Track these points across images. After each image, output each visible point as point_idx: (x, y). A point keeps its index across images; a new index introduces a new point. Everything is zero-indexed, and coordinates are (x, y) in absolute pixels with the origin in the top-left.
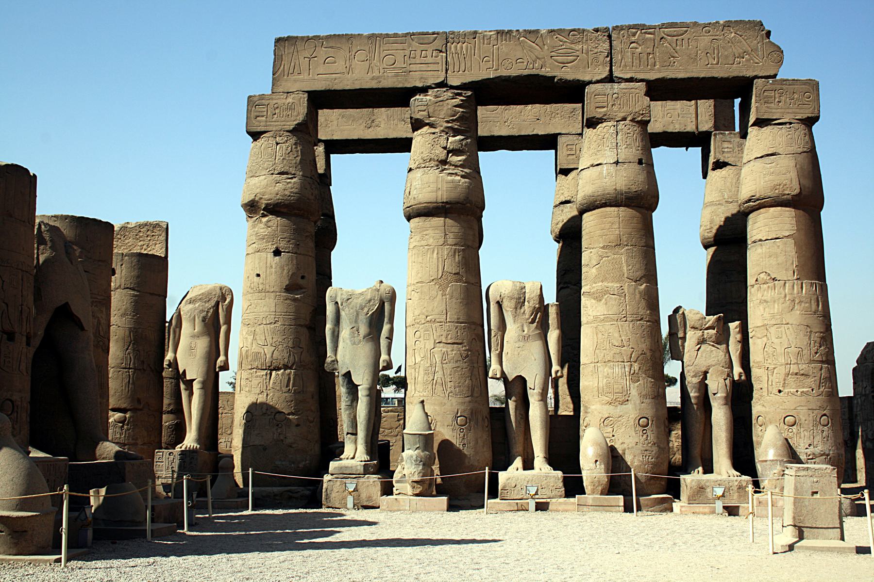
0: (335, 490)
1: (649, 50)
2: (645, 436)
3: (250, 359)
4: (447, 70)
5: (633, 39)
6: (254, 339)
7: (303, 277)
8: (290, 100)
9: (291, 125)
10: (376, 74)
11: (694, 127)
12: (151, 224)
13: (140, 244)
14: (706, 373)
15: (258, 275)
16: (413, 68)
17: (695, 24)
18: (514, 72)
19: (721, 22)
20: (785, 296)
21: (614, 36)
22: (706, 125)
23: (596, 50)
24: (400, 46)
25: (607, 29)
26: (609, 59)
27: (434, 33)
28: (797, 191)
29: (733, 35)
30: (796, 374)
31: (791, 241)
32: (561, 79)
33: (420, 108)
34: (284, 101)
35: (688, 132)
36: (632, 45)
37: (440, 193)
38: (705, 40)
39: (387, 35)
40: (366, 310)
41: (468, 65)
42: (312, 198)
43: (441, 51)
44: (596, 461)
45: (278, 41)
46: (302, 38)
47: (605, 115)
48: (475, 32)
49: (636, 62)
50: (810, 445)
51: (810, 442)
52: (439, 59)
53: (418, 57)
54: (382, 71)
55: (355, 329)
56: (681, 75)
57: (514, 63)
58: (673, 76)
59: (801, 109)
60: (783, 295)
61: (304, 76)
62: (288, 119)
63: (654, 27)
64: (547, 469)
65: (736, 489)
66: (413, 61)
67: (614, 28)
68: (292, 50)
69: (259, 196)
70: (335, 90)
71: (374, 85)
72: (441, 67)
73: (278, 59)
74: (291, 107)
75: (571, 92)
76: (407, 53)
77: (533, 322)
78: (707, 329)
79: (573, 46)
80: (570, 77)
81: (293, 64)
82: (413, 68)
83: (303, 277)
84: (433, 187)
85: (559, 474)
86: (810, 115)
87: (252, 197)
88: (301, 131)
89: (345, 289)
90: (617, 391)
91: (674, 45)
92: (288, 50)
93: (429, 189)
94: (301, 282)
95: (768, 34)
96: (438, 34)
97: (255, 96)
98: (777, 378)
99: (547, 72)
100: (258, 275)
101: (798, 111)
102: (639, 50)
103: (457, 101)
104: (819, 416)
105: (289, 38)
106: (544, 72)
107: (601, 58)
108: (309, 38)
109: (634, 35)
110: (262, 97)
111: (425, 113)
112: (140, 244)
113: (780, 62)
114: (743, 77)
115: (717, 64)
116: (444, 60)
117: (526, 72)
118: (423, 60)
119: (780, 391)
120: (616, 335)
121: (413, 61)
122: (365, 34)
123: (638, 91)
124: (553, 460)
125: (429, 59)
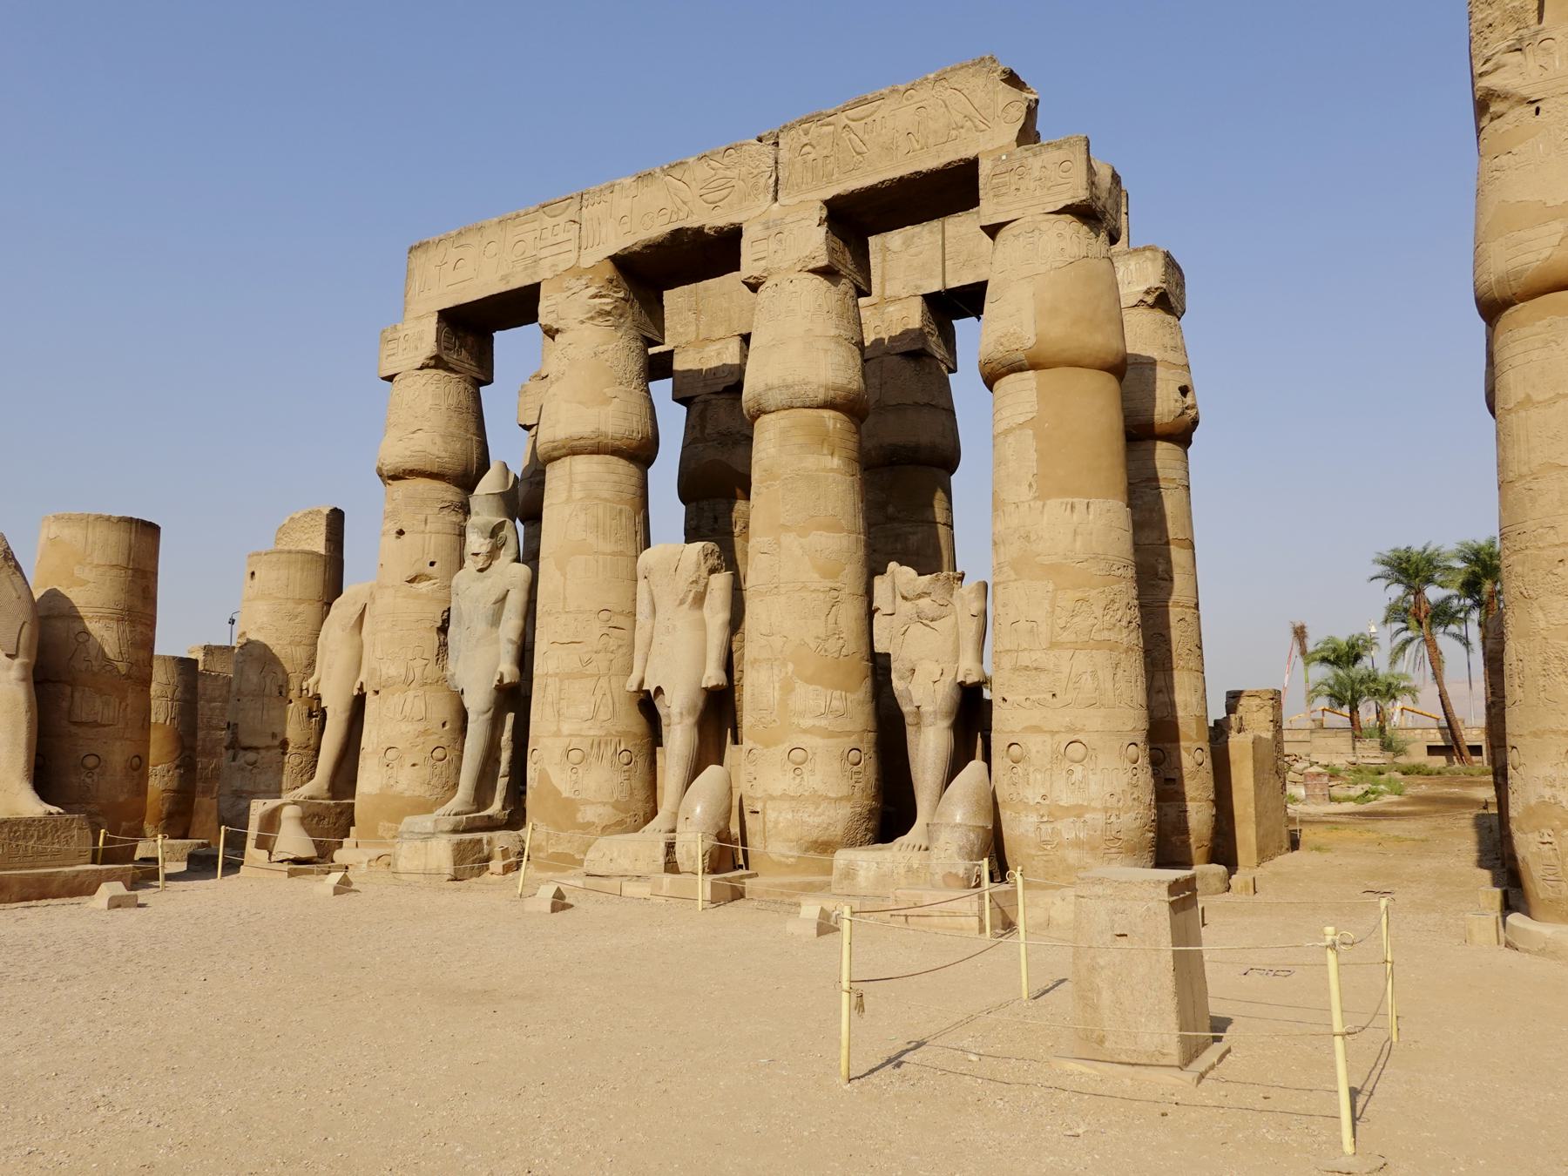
1: (825, 153)
16: (545, 253)
50: (1044, 797)
51: (1043, 792)
72: (573, 246)
77: (682, 602)
78: (919, 596)
79: (728, 173)
103: (593, 291)
109: (806, 134)
121: (543, 243)
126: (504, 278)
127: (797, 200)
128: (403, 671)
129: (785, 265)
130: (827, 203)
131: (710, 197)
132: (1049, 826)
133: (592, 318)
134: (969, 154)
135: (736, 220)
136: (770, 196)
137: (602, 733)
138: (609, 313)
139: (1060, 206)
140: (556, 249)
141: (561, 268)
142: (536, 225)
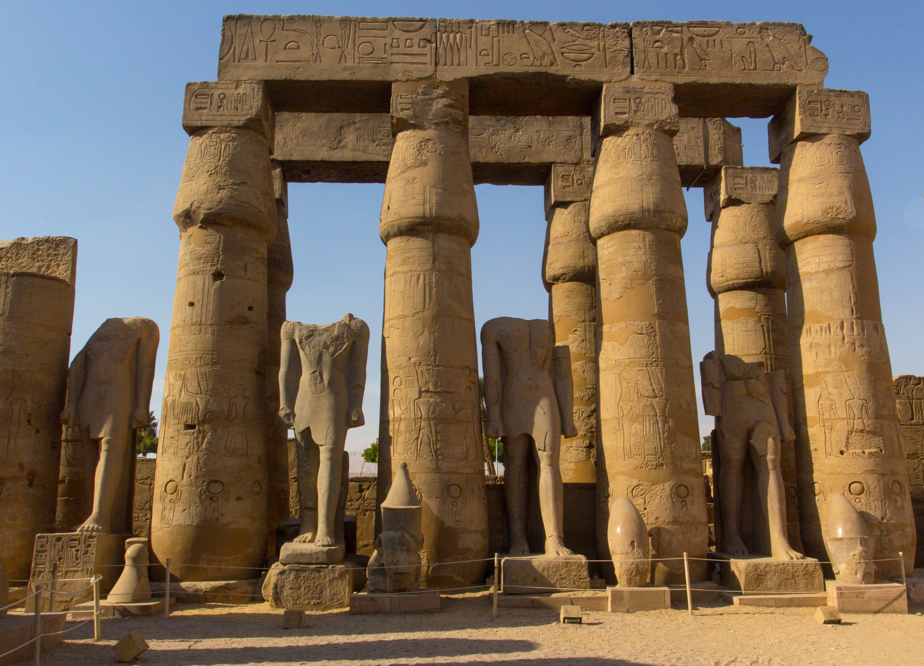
0: (288, 586)
2: (684, 509)
3: (177, 411)
4: (436, 64)
5: (657, 37)
6: (184, 385)
7: (250, 308)
8: (241, 90)
9: (240, 120)
10: (350, 63)
11: (703, 161)
12: (53, 240)
13: (37, 264)
14: (749, 434)
15: (192, 304)
16: (396, 58)
17: (728, 24)
18: (518, 68)
19: (758, 23)
20: (844, 338)
21: (635, 33)
22: (715, 160)
23: (614, 48)
24: (381, 33)
25: (626, 26)
26: (629, 59)
27: (421, 20)
28: (854, 214)
29: (771, 38)
30: (862, 431)
31: (846, 273)
32: (573, 79)
33: (404, 106)
34: (233, 91)
35: (696, 166)
36: (657, 44)
37: (427, 207)
38: (738, 45)
39: (364, 20)
40: (331, 349)
41: (462, 58)
42: (264, 210)
43: (429, 41)
44: (633, 542)
45: (228, 19)
46: (258, 18)
47: (626, 122)
48: (472, 21)
49: (662, 63)
52: (426, 50)
53: (402, 45)
54: (357, 61)
55: (317, 373)
56: (714, 80)
57: (518, 58)
58: (705, 81)
59: (850, 124)
60: (841, 337)
61: (260, 62)
62: (237, 113)
63: (682, 26)
64: (565, 553)
65: (801, 574)
66: (395, 50)
67: (637, 24)
68: (244, 31)
69: (196, 204)
70: (298, 81)
71: (346, 76)
73: (227, 41)
74: (241, 100)
75: (582, 100)
76: (389, 40)
79: (587, 42)
80: (584, 77)
81: (245, 48)
82: (396, 58)
83: (250, 308)
84: (420, 198)
85: (582, 559)
86: (860, 131)
87: (187, 206)
88: (253, 129)
89: (304, 322)
90: (649, 452)
91: (705, 46)
92: (242, 30)
93: (413, 202)
94: (248, 314)
95: (810, 38)
96: (425, 21)
97: (195, 84)
98: (838, 437)
99: (558, 69)
100: (192, 304)
101: (845, 126)
102: (665, 49)
104: (890, 483)
105: (240, 18)
106: (552, 70)
107: (620, 57)
108: (266, 19)
109: (659, 32)
110: (205, 84)
111: (410, 112)
112: (37, 264)
113: (825, 70)
114: (785, 85)
115: (755, 69)
116: (434, 51)
117: (532, 70)
118: (408, 51)
119: (842, 453)
120: (647, 383)
121: (395, 50)
122: (336, 17)
123: (664, 96)
124: (569, 540)
125: (415, 50)
126: (345, 69)
127: (654, 78)
128: (226, 407)
129: (647, 122)
130: (677, 88)
131: (572, 56)
132: (887, 539)
133: (447, 123)
134: (790, 82)
135: (596, 77)
136: (628, 69)
137: (472, 471)
138: (460, 123)
139: (856, 132)
140: (409, 59)
141: (416, 75)
142: (386, 33)
